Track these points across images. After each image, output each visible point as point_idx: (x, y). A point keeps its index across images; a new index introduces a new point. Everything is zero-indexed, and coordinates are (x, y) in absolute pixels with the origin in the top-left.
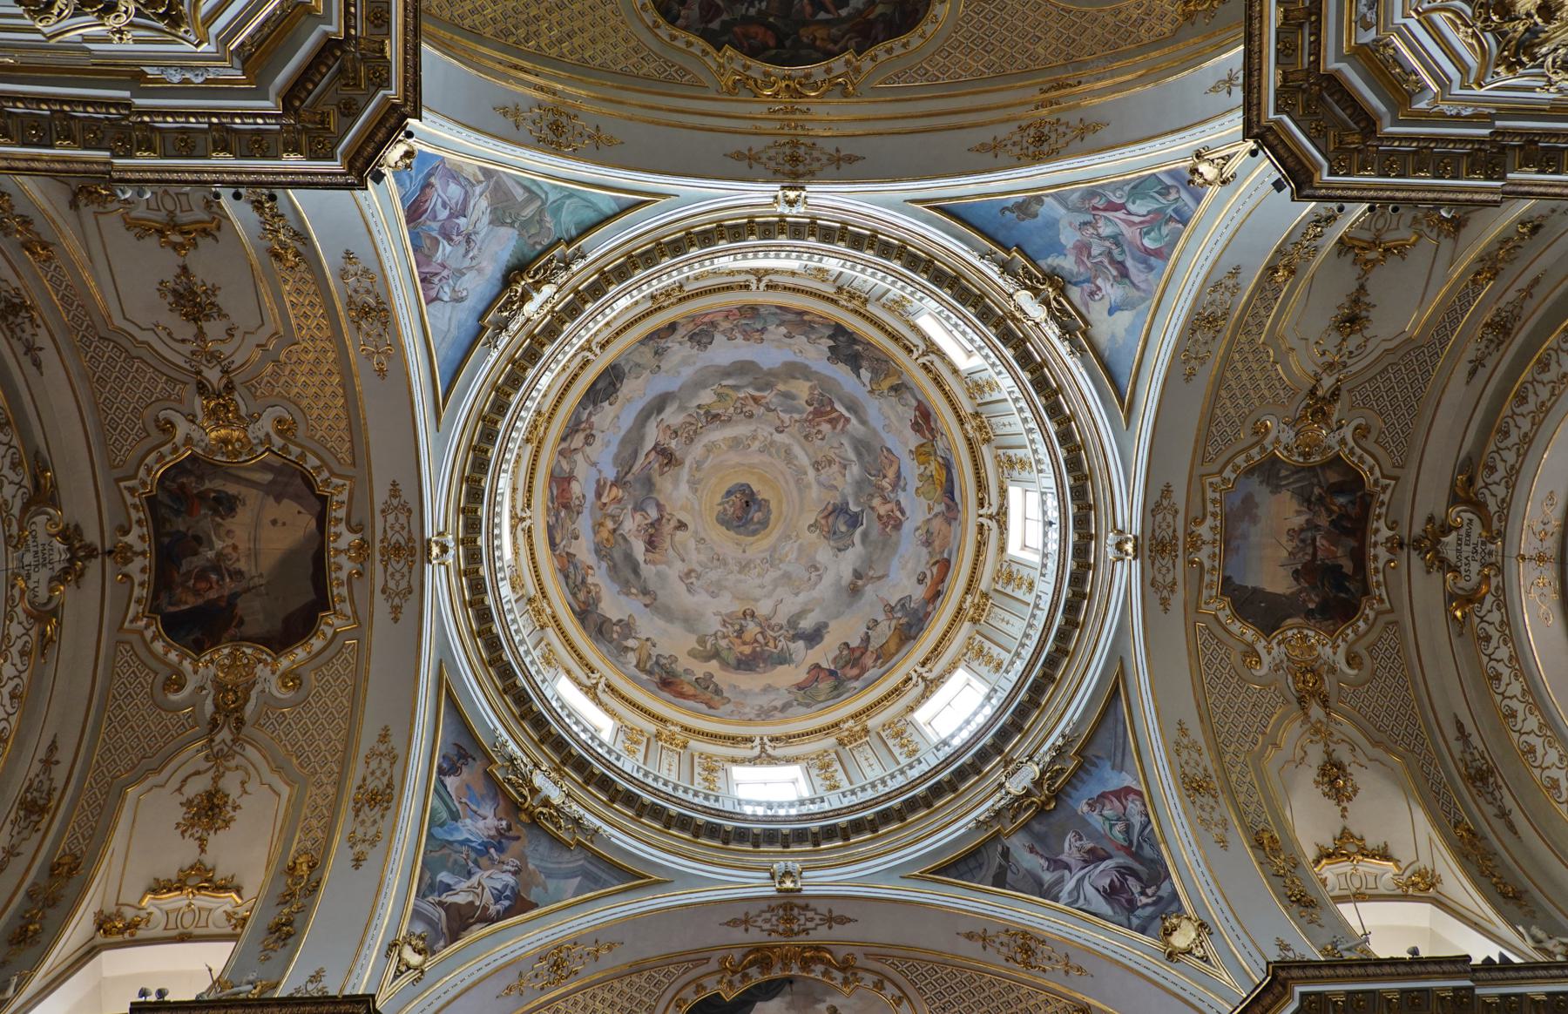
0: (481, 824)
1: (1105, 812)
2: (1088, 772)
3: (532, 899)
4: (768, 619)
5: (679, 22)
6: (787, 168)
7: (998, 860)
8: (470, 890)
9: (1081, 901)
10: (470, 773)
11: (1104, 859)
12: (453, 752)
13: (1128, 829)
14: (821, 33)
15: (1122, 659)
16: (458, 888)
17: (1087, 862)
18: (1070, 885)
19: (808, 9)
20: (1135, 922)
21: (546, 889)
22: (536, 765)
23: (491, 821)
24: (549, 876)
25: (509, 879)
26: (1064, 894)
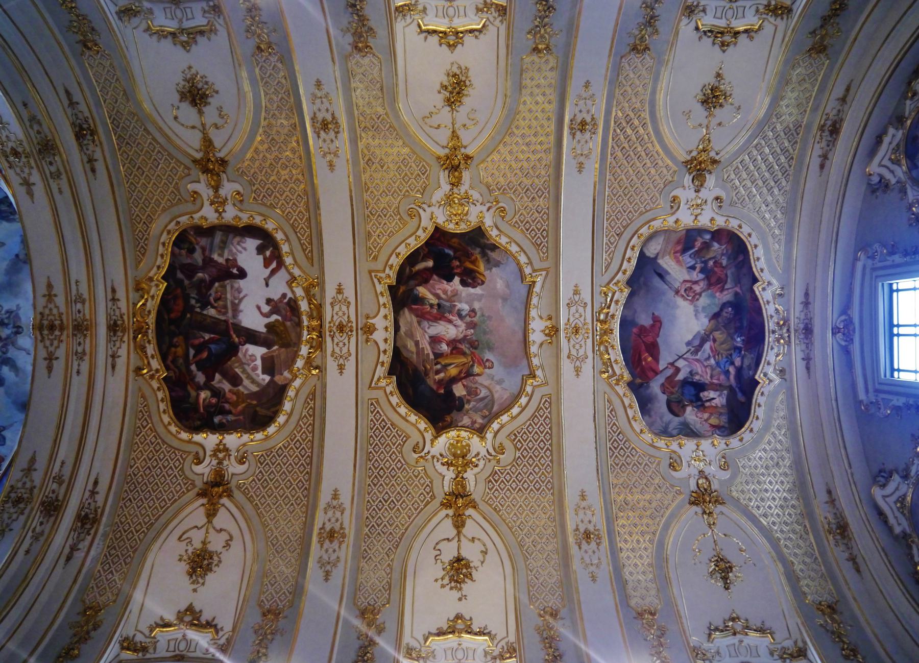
4: (14, 344)
5: (176, 249)
6: (45, 323)
14: (180, 351)
19: (197, 342)
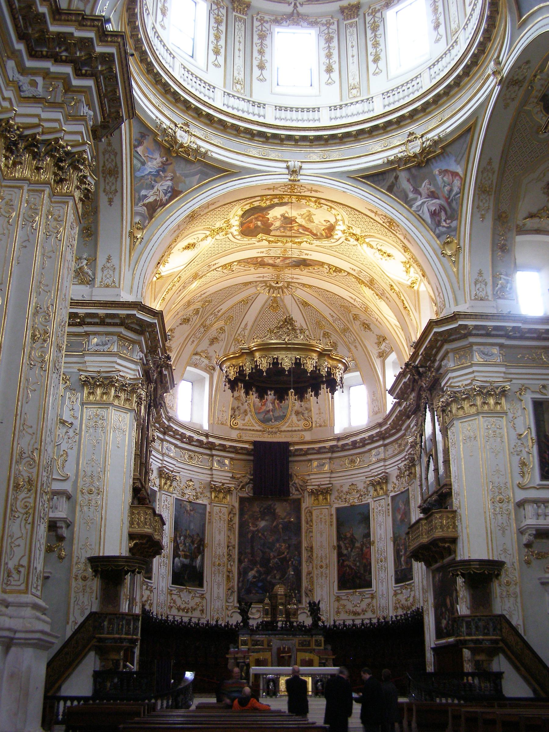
0: (154, 163)
1: (445, 179)
2: (444, 158)
3: (180, 189)
7: (392, 179)
8: (154, 194)
9: (421, 212)
10: (148, 142)
11: (436, 198)
12: (138, 136)
13: (451, 191)
15: (477, 118)
16: (149, 195)
17: (429, 196)
18: (419, 203)
20: (437, 231)
21: (185, 183)
22: (176, 125)
23: (159, 160)
24: (186, 176)
25: (169, 183)
26: (415, 206)
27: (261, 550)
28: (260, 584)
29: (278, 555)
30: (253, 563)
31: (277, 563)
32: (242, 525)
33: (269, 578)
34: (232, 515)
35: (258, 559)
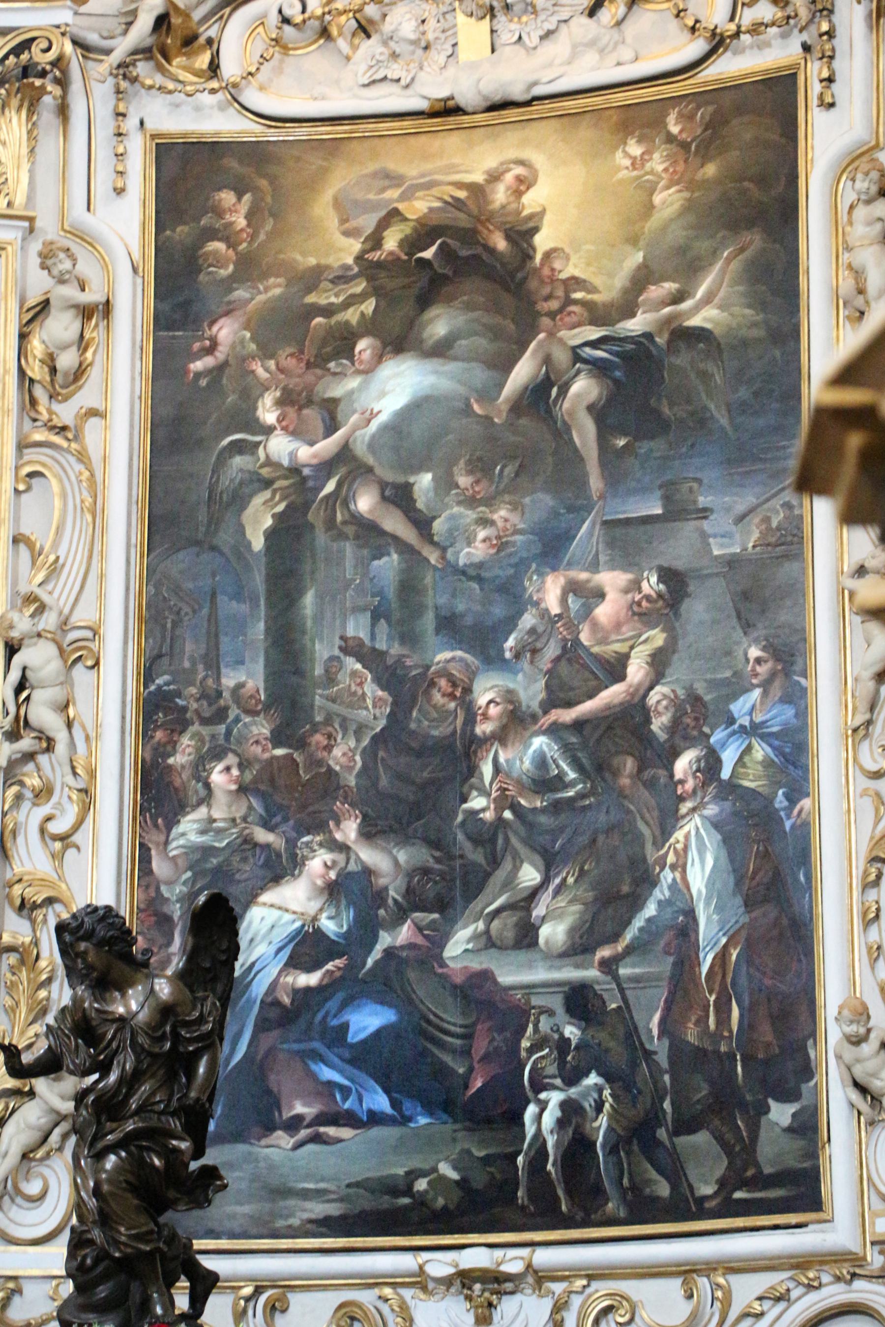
27: (370, 657)
28: (367, 1021)
29: (558, 698)
30: (295, 799)
31: (544, 782)
32: (187, 427)
33: (459, 946)
34: (60, 327)
35: (344, 755)
